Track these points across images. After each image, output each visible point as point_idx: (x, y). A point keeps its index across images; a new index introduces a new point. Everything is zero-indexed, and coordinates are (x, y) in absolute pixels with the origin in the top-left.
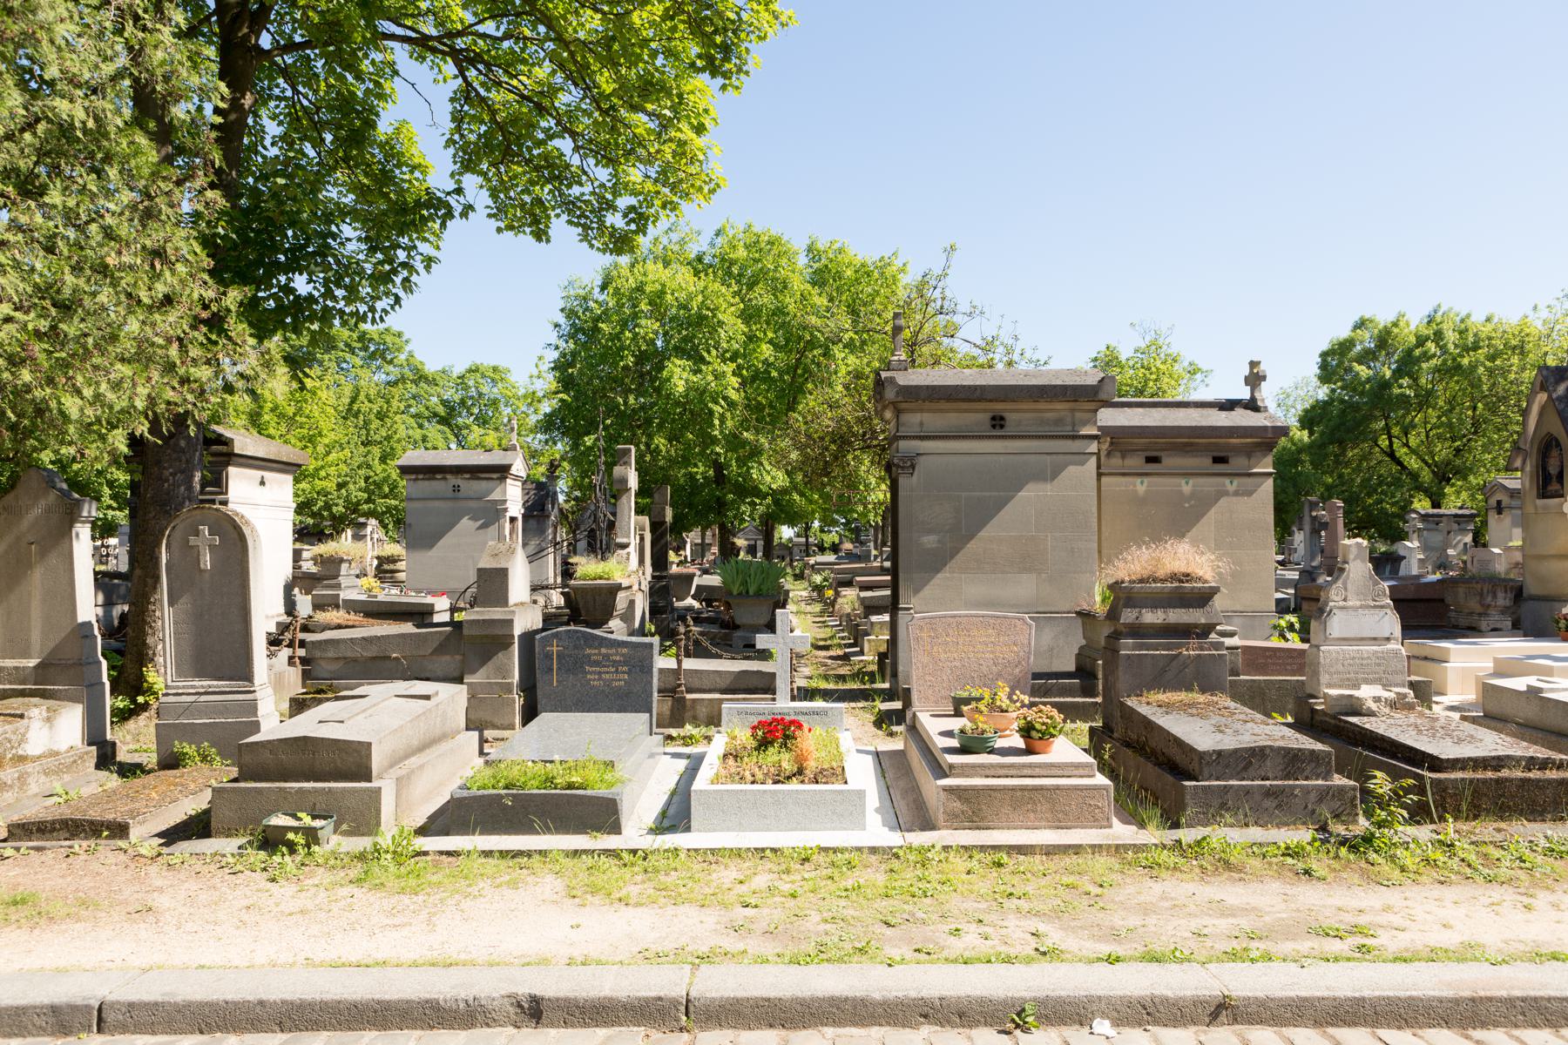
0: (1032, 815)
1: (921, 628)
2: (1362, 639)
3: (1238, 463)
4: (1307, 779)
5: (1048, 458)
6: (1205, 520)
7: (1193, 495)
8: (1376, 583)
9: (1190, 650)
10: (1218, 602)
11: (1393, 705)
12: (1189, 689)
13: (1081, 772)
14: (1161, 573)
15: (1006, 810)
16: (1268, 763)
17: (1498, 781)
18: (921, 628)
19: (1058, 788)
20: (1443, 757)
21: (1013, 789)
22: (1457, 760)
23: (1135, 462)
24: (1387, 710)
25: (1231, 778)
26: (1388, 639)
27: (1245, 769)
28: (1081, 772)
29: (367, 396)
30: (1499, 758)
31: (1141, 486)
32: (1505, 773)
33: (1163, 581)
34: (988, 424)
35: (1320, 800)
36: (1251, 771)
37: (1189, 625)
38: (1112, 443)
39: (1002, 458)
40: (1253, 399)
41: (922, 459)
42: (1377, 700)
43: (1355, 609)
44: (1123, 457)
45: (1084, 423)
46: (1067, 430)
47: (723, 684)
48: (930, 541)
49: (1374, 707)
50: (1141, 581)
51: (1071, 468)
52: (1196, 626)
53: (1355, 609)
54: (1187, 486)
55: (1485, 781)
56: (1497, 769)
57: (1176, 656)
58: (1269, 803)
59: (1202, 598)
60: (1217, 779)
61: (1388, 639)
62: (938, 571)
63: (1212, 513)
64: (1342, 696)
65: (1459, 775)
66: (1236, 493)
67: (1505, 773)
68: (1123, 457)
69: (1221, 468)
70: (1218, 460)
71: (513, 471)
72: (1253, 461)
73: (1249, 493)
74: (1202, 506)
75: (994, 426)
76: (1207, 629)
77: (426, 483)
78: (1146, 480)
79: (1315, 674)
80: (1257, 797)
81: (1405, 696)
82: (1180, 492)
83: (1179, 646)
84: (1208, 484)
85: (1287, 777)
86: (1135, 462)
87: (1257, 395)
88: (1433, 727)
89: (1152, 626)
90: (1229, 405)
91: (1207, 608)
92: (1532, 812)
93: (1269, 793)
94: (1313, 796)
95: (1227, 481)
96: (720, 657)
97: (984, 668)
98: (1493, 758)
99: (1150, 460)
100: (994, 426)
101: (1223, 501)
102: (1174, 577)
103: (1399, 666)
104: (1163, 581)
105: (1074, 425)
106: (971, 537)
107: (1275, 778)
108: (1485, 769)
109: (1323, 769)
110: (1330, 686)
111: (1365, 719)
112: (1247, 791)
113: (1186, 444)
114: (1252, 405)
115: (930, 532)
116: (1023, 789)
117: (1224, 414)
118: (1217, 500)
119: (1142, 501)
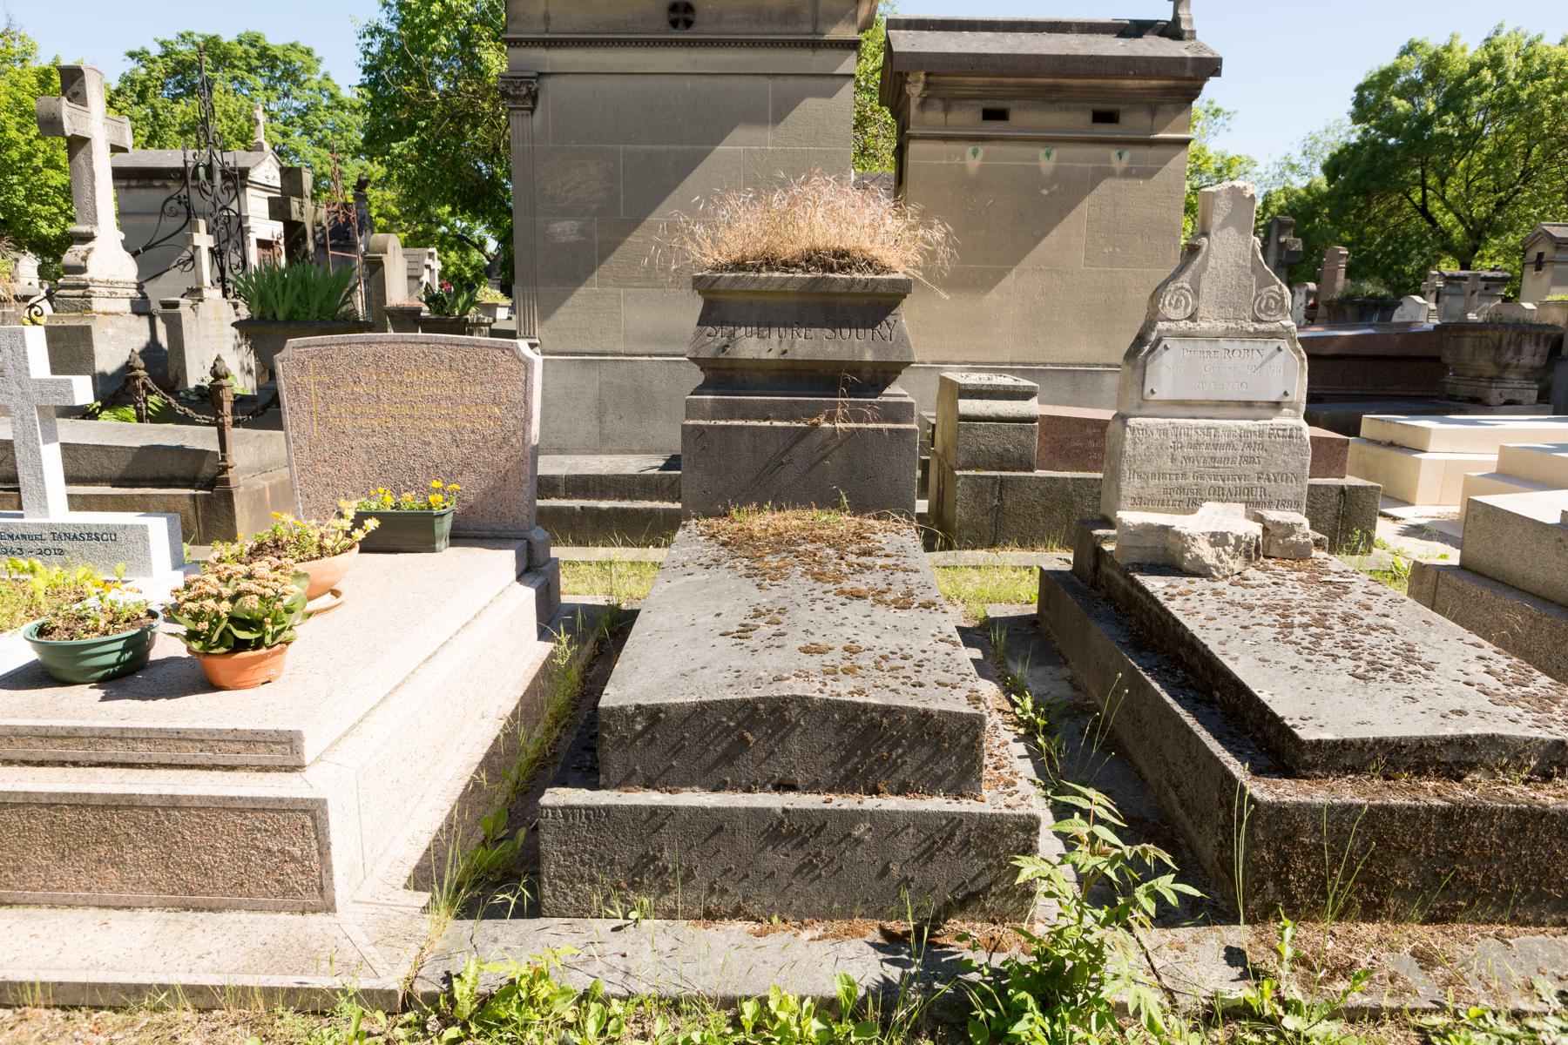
0: (112, 874)
1: (303, 368)
2: (1221, 404)
3: (1133, 122)
4: (902, 790)
5: (770, 82)
6: (1072, 217)
7: (1056, 175)
8: (1264, 282)
9: (837, 420)
10: (907, 316)
11: (1253, 552)
12: (829, 502)
13: (263, 756)
14: (788, 251)
15: (40, 857)
16: (795, 745)
17: (1451, 817)
18: (303, 368)
19: (173, 804)
20: (1307, 733)
21: (52, 803)
22: (1343, 746)
23: (966, 118)
24: (1237, 565)
25: (688, 782)
26: (1277, 405)
27: (728, 758)
28: (263, 756)
29: (225, 113)
30: (1465, 743)
31: (972, 158)
32: (1471, 791)
33: (787, 265)
34: (664, 22)
35: (927, 854)
36: (745, 766)
37: (839, 365)
38: (928, 85)
39: (688, 83)
40: (1176, 19)
41: (548, 83)
42: (1218, 539)
43: (1213, 337)
44: (947, 109)
45: (835, 19)
46: (804, 31)
47: (117, 467)
48: (565, 230)
49: (1208, 554)
50: (739, 265)
51: (810, 104)
52: (855, 367)
53: (1213, 337)
54: (1047, 161)
55: (1410, 815)
56: (1453, 772)
57: (804, 433)
58: (780, 859)
59: (875, 304)
60: (649, 784)
61: (1277, 405)
62: (579, 280)
63: (1085, 206)
64: (1147, 529)
65: (1346, 792)
66: (1127, 174)
67: (1471, 791)
68: (947, 109)
69: (1105, 130)
70: (1103, 117)
71: (256, 175)
72: (1158, 119)
73: (1148, 174)
74: (1070, 191)
75: (674, 24)
76: (886, 373)
77: (143, 192)
78: (982, 149)
79: (1115, 475)
80: (746, 843)
81: (1290, 529)
82: (1037, 170)
83: (813, 411)
84: (1082, 157)
85: (846, 784)
86: (966, 118)
87: (1183, 13)
88: (1311, 633)
89: (758, 365)
90: (1137, 29)
91: (882, 328)
92: (1535, 900)
93: (778, 829)
94: (907, 844)
95: (1113, 153)
96: (191, 421)
97: (435, 452)
98: (1448, 742)
99: (989, 115)
100: (674, 24)
101: (1105, 186)
102: (812, 258)
103: (1294, 464)
104: (787, 265)
105: (816, 22)
106: (635, 223)
107: (813, 787)
108: (1420, 770)
109: (950, 764)
110: (1140, 503)
111: (1182, 583)
112: (716, 825)
113: (1052, 88)
114: (1172, 30)
115: (566, 214)
116: (80, 803)
117: (1121, 41)
118: (1094, 184)
119: (972, 184)
